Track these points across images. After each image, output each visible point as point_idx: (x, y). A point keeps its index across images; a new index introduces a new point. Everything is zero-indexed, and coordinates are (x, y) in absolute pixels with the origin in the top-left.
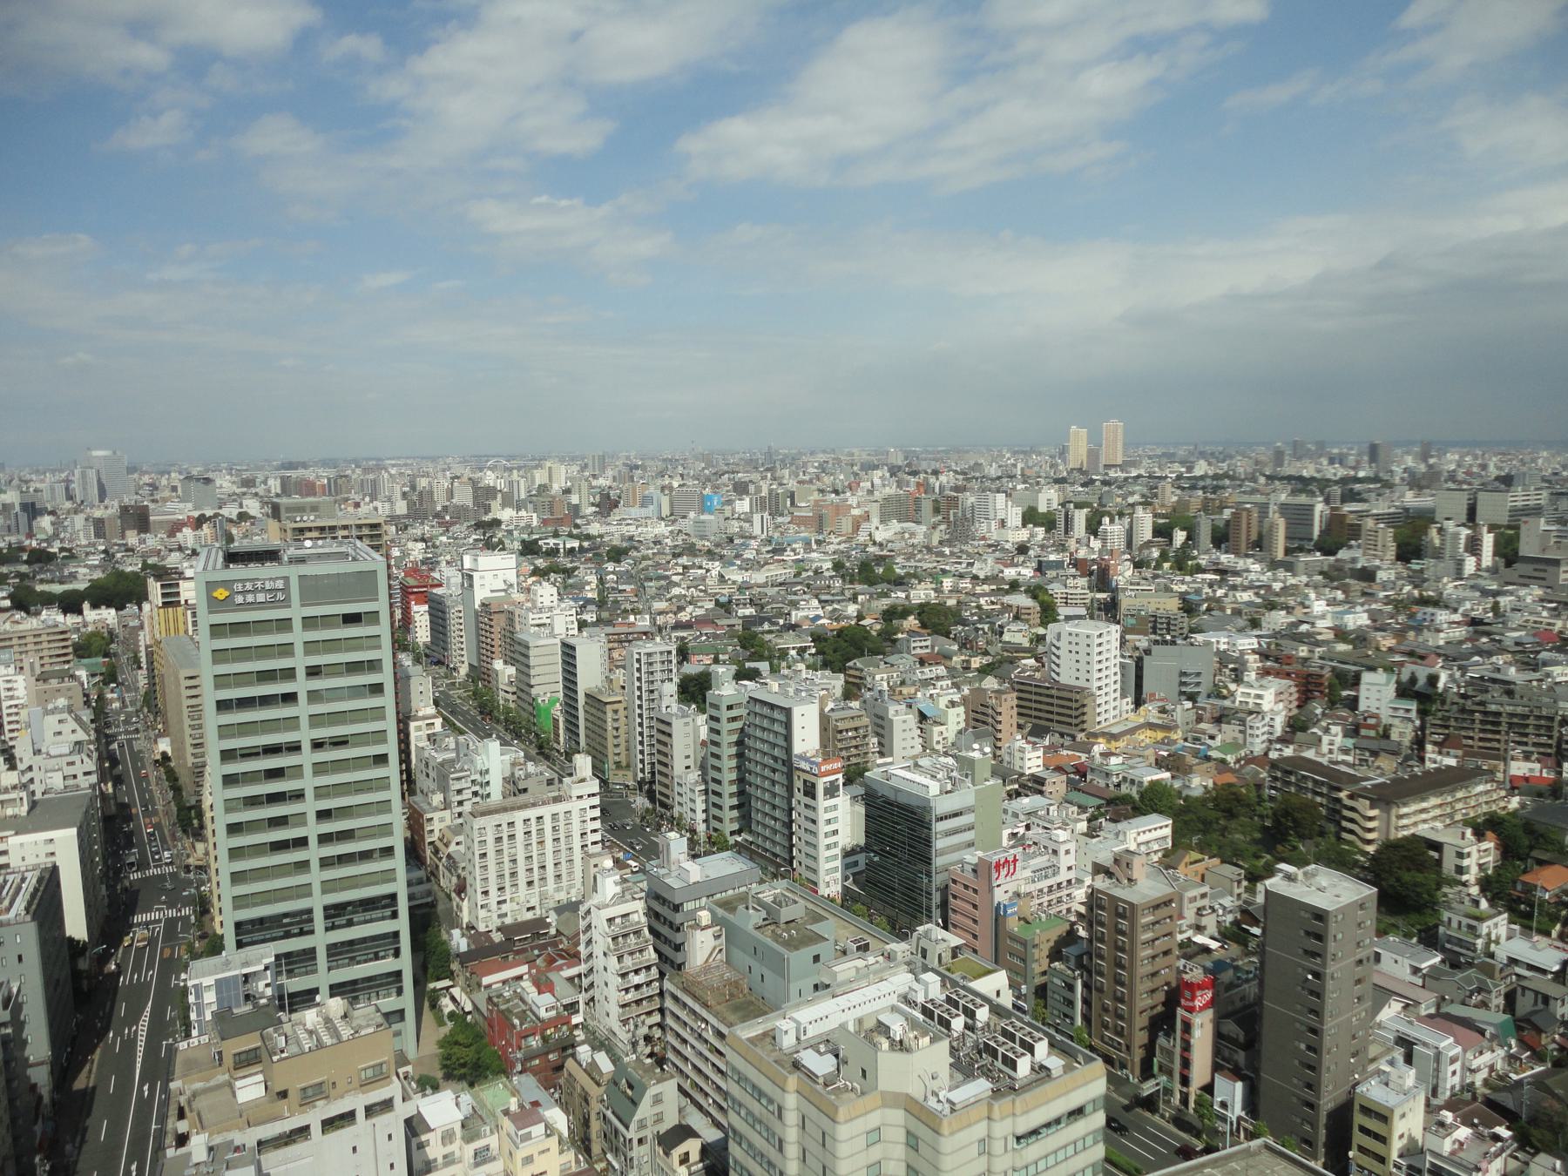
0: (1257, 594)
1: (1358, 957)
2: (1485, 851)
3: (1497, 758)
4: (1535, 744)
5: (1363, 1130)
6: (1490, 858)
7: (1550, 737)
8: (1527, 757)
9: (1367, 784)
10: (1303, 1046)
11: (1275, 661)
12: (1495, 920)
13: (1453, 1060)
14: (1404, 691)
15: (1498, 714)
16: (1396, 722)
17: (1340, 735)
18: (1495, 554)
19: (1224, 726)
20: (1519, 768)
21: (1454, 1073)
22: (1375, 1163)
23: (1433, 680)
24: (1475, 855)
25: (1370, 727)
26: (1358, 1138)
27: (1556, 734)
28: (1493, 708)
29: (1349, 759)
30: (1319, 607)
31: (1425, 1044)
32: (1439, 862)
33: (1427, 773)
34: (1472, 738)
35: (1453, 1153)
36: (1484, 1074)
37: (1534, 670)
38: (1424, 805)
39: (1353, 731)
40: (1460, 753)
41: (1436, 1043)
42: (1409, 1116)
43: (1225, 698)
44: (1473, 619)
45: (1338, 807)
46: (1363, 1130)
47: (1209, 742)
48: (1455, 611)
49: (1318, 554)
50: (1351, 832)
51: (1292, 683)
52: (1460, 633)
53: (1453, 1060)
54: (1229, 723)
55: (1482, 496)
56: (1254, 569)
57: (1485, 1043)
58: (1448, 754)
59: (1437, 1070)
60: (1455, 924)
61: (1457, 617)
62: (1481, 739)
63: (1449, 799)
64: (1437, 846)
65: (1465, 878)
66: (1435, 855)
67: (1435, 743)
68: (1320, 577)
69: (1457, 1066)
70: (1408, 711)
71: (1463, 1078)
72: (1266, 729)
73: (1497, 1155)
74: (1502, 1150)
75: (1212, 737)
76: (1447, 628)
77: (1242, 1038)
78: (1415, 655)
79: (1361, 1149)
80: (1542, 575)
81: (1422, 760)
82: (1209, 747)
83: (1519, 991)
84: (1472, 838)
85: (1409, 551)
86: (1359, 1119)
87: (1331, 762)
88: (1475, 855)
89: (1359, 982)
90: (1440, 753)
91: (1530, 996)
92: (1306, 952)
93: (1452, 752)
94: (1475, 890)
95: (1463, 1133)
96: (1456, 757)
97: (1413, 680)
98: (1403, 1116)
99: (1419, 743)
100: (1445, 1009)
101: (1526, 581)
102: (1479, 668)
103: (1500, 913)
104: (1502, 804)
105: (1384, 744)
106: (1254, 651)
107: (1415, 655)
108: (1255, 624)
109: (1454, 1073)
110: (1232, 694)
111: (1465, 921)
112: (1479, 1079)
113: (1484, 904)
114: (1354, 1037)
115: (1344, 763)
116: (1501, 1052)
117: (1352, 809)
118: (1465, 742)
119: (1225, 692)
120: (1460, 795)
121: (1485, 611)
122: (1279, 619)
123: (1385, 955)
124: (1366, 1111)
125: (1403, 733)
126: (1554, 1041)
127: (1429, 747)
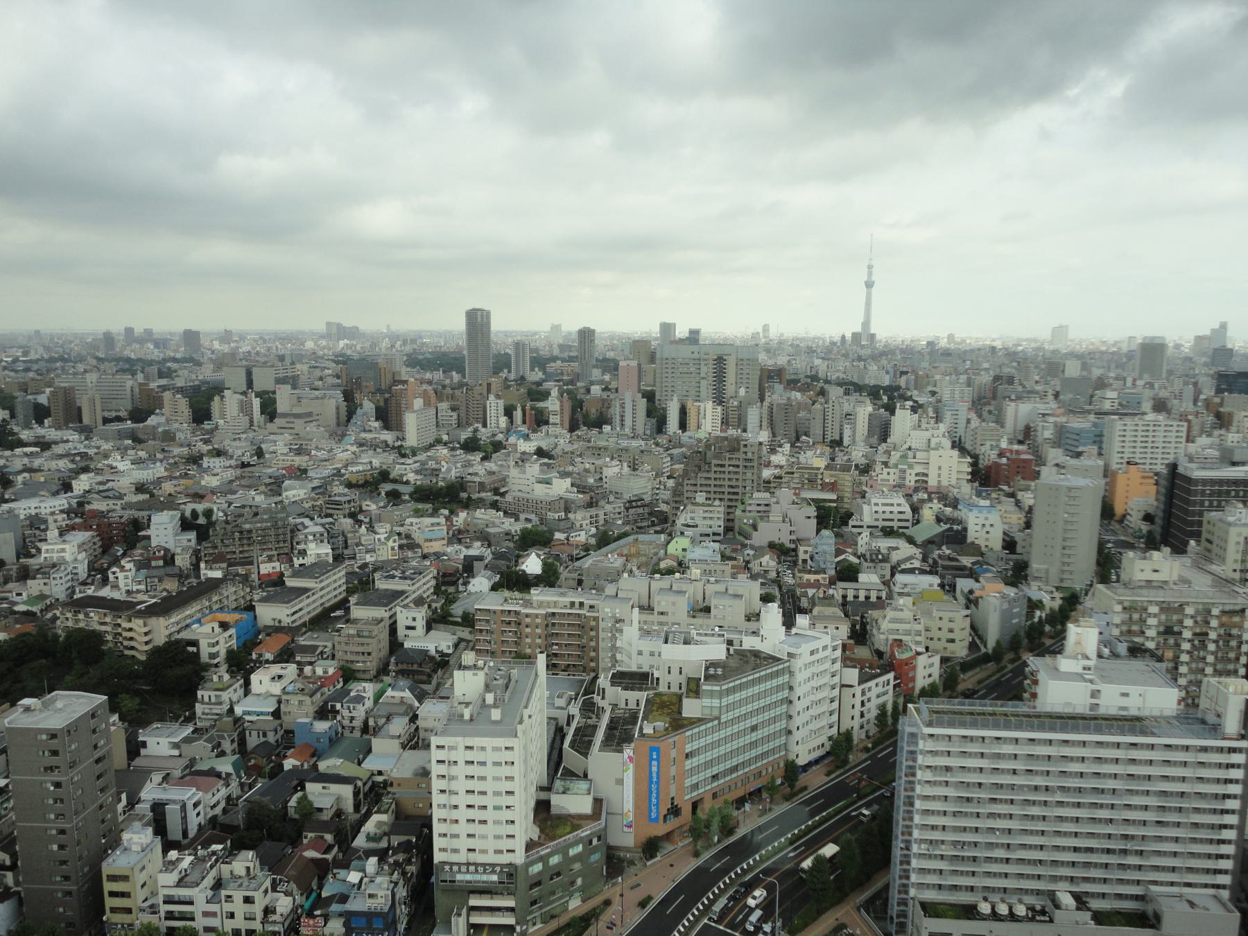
0: (73, 461)
1: (96, 757)
2: (230, 636)
3: (251, 563)
4: (276, 549)
5: (113, 894)
6: (235, 641)
7: (284, 542)
8: (270, 559)
9: (142, 607)
10: (55, 847)
11: (79, 515)
12: (234, 687)
13: (196, 805)
14: (186, 524)
15: (250, 531)
16: (179, 550)
17: (134, 569)
18: (262, 413)
19: (29, 582)
20: (266, 568)
21: (198, 814)
22: (125, 916)
23: (208, 513)
24: (222, 642)
25: (158, 558)
26: (110, 902)
27: (289, 538)
28: (247, 526)
29: (142, 587)
30: (123, 465)
31: (174, 802)
32: (197, 654)
33: (200, 584)
34: (234, 552)
35: (181, 880)
36: (223, 804)
37: (280, 495)
38: (188, 613)
39: (142, 565)
40: (225, 565)
41: (181, 798)
42: (150, 869)
43: (33, 556)
44: (243, 463)
45: (120, 630)
46: (113, 894)
47: (18, 599)
48: (232, 457)
49: (129, 422)
50: (132, 648)
51: (95, 534)
52: (230, 474)
53: (196, 805)
54: (34, 578)
55: (255, 371)
56: (72, 439)
57: (222, 782)
58: (216, 569)
59: (184, 818)
60: (206, 699)
61: (233, 462)
62: (241, 552)
63: (207, 604)
64: (194, 643)
65: (216, 661)
66: (191, 649)
67: (206, 562)
68: (130, 442)
69: (200, 808)
70: (190, 540)
71: (206, 814)
72: (69, 577)
73: (212, 867)
74: (217, 861)
75: (19, 594)
76: (215, 474)
77: (8, 863)
78: (198, 497)
79: (113, 910)
80: (288, 425)
81: (198, 576)
82: (15, 603)
83: (247, 732)
84: (220, 630)
85: (201, 415)
86: (108, 886)
87: (128, 592)
88: (222, 642)
89: (99, 777)
90: (211, 569)
91: (254, 733)
92: (46, 769)
93: (217, 565)
94: (224, 668)
95: (188, 860)
96: (220, 568)
97: (195, 514)
98: (144, 868)
99: (196, 567)
100: (198, 767)
101: (283, 431)
102: (239, 498)
103: (238, 680)
104: (248, 598)
105: (169, 570)
106: (62, 511)
107: (198, 497)
108: (67, 487)
109: (198, 814)
110: (39, 550)
111: (213, 694)
112: (218, 810)
113: (226, 677)
114: (103, 821)
115: (138, 591)
116: (234, 784)
117: (130, 630)
118: (229, 557)
119: (33, 551)
120: (215, 598)
121: (252, 456)
122: (82, 484)
123: (151, 741)
124: (113, 878)
125: (183, 561)
126: (271, 761)
127: (202, 565)
